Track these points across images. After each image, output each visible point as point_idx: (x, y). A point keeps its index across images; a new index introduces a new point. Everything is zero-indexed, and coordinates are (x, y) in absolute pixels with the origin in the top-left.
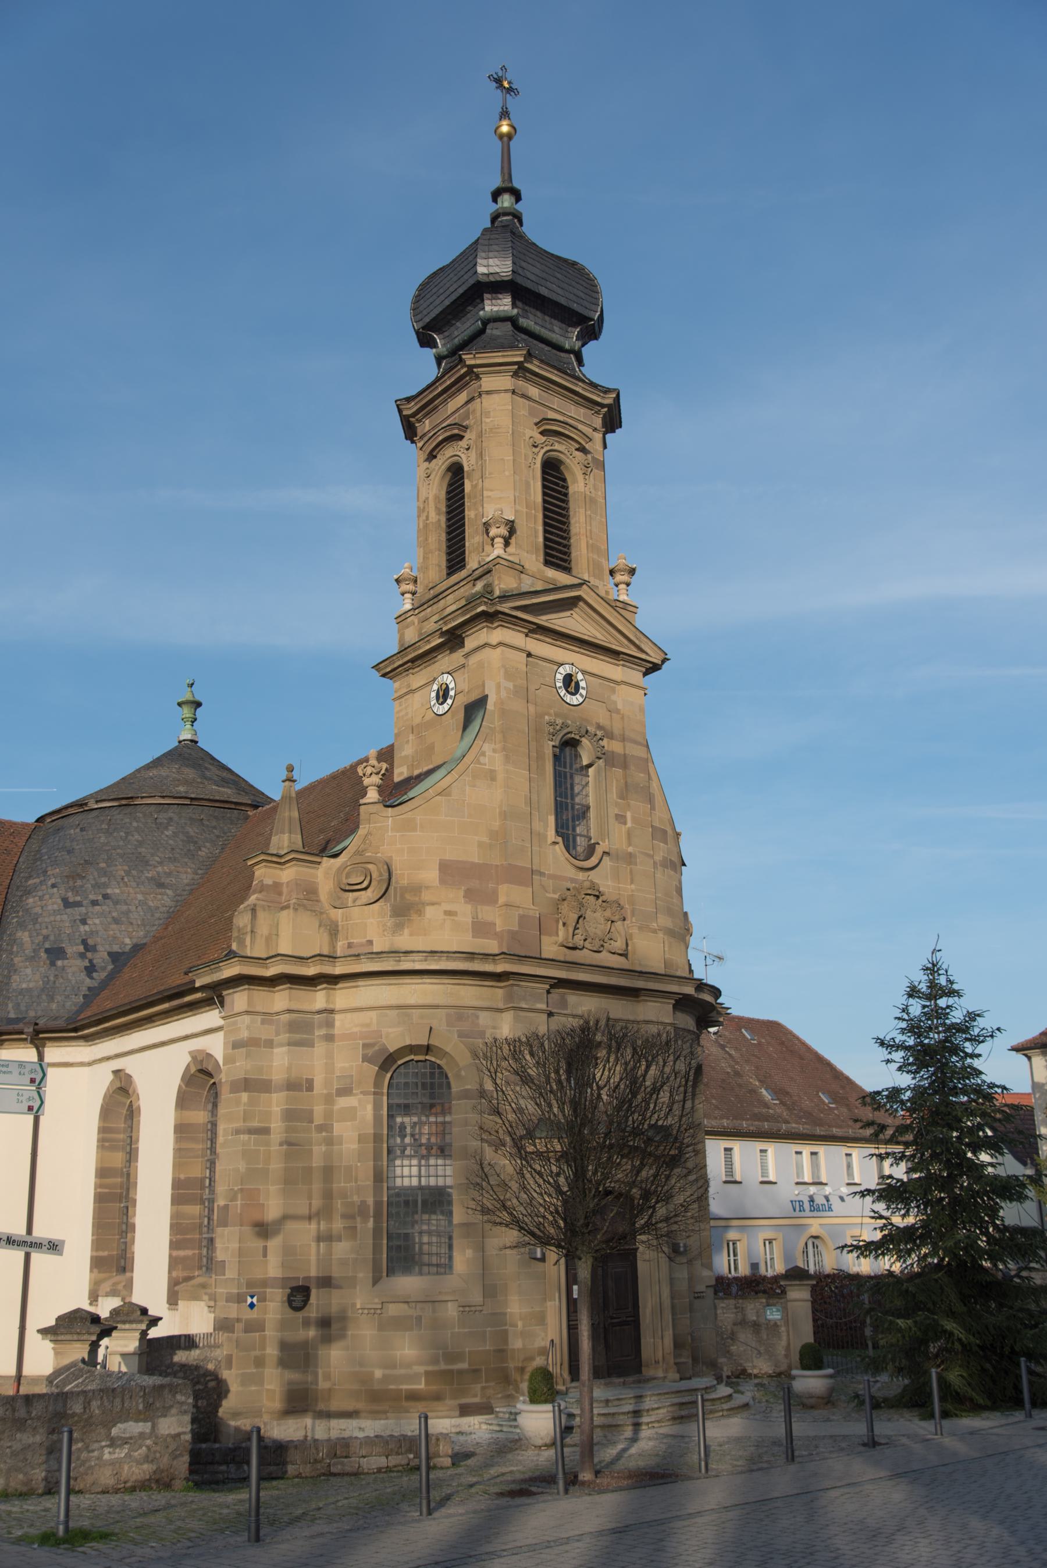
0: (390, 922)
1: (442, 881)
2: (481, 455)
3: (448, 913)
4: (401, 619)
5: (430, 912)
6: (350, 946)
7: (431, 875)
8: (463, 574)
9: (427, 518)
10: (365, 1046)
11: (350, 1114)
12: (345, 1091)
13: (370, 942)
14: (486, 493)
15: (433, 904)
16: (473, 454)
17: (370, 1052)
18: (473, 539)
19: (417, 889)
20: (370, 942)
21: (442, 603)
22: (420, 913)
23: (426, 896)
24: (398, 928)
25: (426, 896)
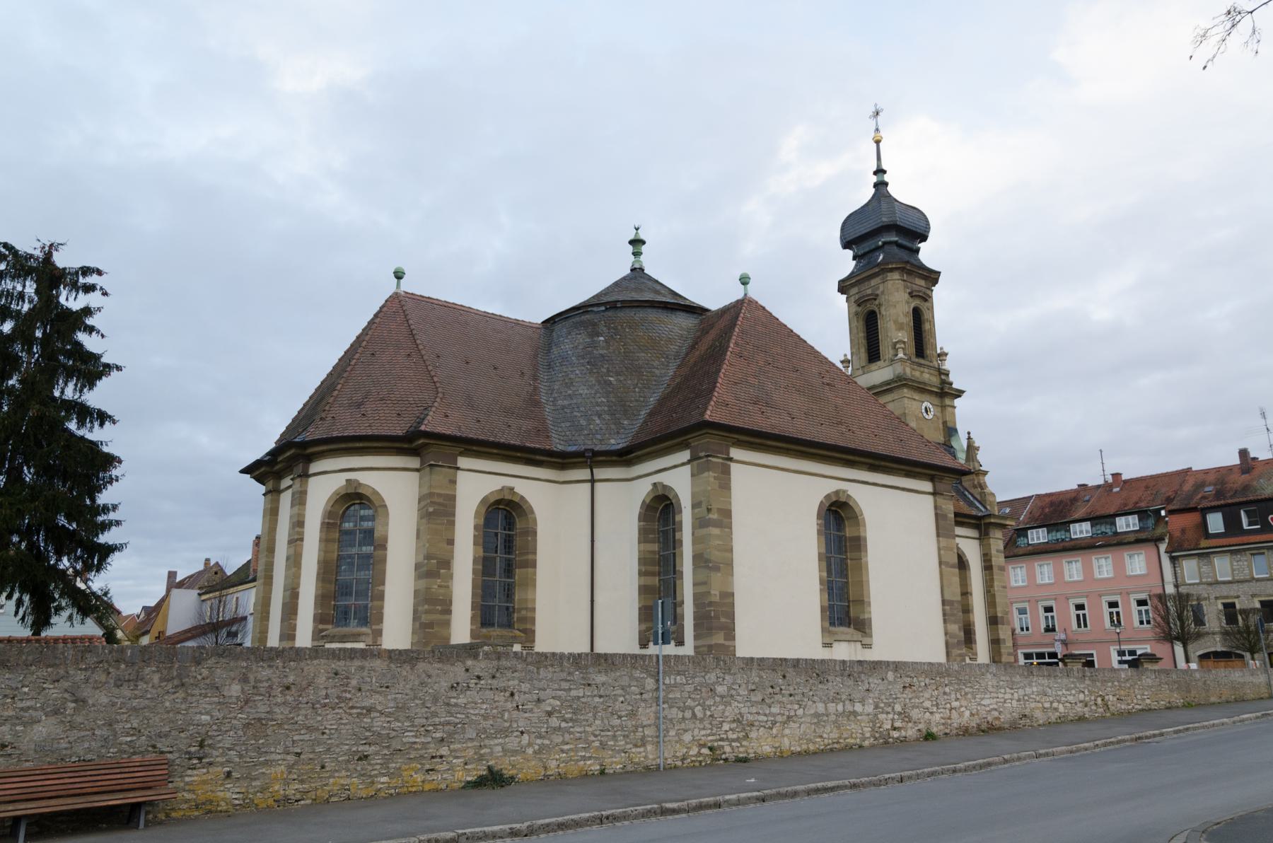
21: (922, 369)
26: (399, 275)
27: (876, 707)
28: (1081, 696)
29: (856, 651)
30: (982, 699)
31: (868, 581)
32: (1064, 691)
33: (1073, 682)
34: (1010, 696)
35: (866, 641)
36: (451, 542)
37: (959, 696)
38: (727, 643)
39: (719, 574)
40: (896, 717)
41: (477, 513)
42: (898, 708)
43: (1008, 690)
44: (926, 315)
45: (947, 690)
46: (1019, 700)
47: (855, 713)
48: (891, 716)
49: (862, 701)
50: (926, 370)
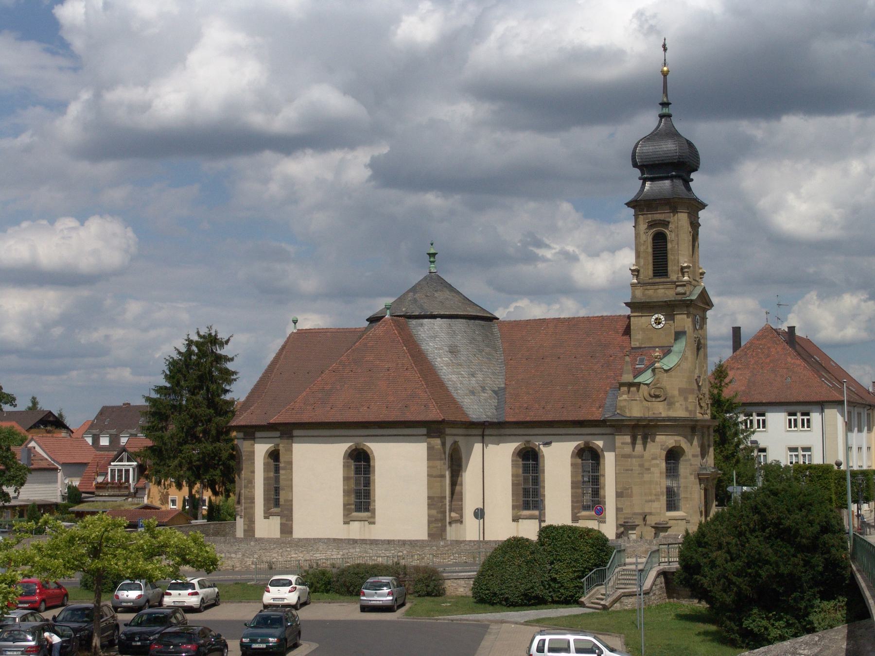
0: (666, 407)
1: (679, 395)
2: (677, 235)
3: (681, 405)
4: (633, 285)
5: (677, 405)
6: (654, 413)
7: (676, 393)
8: (668, 280)
9: (647, 248)
10: (661, 445)
11: (657, 465)
12: (655, 458)
13: (661, 413)
14: (679, 252)
15: (678, 402)
16: (673, 235)
17: (664, 447)
18: (672, 268)
19: (673, 397)
20: (661, 413)
21: (657, 287)
22: (675, 405)
23: (676, 399)
24: (669, 409)
25: (676, 399)
26: (295, 322)
27: (243, 555)
28: (400, 554)
29: (364, 525)
30: (314, 554)
31: (375, 490)
32: (383, 551)
33: (394, 547)
34: (336, 553)
35: (371, 520)
36: (253, 472)
37: (297, 552)
38: (287, 522)
39: (284, 492)
40: (255, 560)
41: (264, 457)
42: (256, 556)
43: (334, 550)
44: (670, 236)
45: (289, 549)
46: (343, 555)
47: (232, 558)
48: (252, 559)
49: (235, 553)
50: (661, 287)
